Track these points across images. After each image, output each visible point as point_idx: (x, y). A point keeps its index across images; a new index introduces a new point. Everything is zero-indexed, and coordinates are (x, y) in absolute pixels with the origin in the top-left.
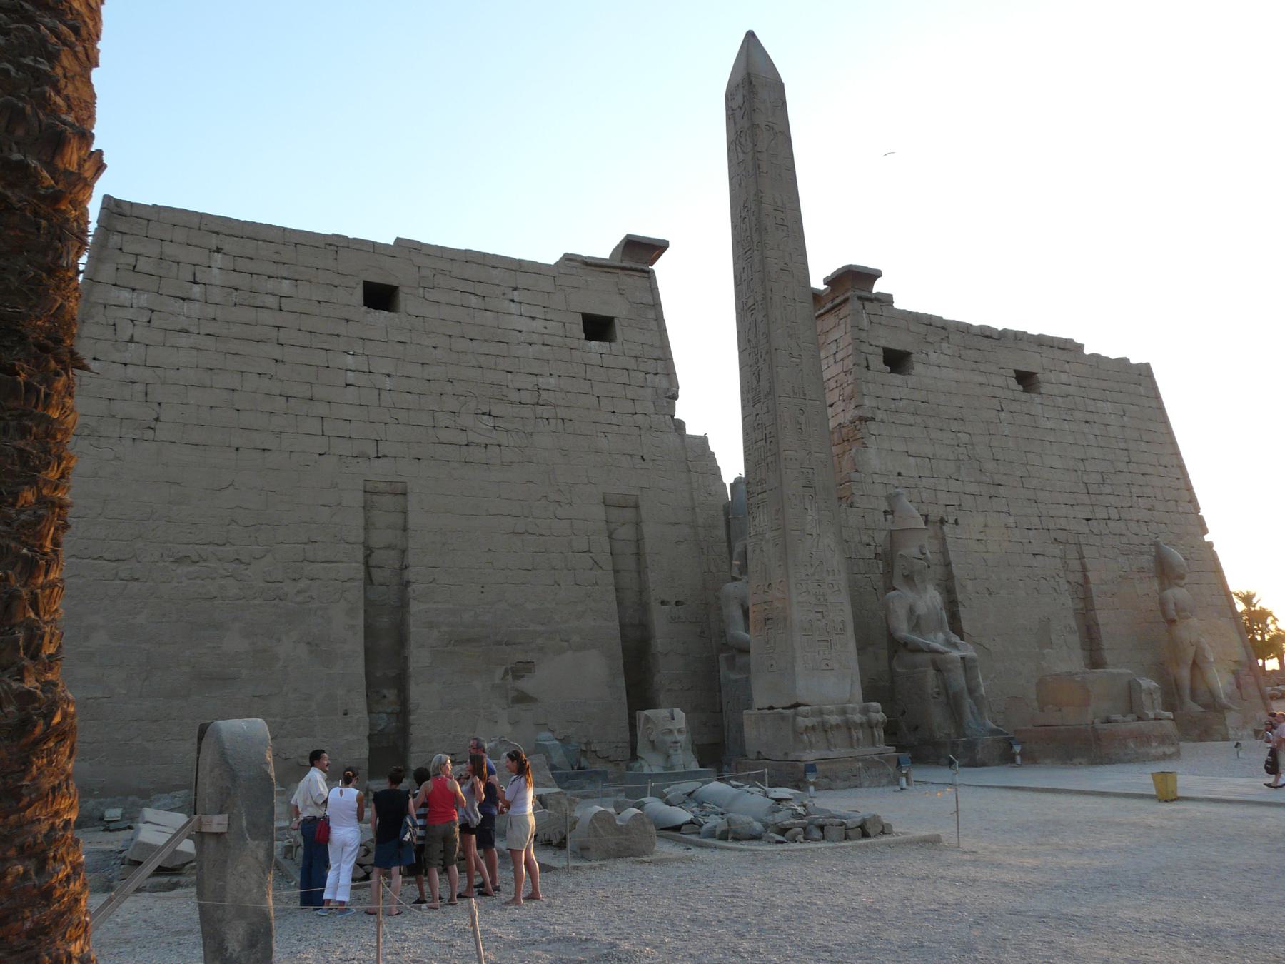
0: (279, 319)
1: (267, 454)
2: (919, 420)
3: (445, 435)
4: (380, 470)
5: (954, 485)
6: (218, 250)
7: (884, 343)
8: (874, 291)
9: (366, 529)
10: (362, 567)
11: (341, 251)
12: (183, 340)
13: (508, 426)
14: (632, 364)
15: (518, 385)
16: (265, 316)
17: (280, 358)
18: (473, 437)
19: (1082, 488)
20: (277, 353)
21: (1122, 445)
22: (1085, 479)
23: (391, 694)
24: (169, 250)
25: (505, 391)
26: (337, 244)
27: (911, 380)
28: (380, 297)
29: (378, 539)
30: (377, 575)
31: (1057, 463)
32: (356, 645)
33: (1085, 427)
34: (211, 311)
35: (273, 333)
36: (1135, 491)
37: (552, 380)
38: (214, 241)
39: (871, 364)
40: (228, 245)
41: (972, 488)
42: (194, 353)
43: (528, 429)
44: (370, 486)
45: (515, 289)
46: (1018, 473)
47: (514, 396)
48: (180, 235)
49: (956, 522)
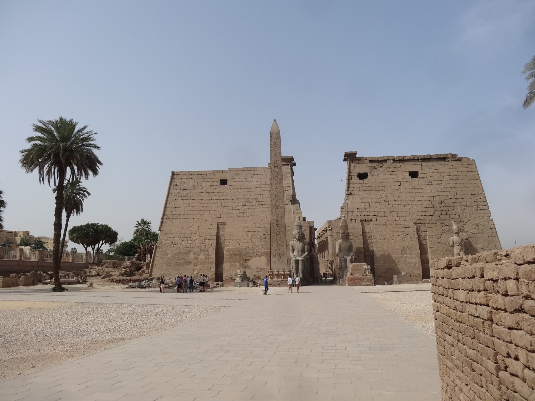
2: (367, 192)
3: (234, 211)
4: (221, 220)
5: (377, 210)
8: (357, 156)
12: (185, 198)
18: (241, 211)
21: (455, 190)
22: (433, 203)
24: (183, 180)
26: (214, 172)
27: (366, 181)
28: (224, 182)
31: (422, 199)
33: (437, 186)
36: (456, 204)
37: (261, 196)
38: (191, 177)
40: (193, 177)
41: (385, 210)
47: (251, 201)
48: (184, 177)
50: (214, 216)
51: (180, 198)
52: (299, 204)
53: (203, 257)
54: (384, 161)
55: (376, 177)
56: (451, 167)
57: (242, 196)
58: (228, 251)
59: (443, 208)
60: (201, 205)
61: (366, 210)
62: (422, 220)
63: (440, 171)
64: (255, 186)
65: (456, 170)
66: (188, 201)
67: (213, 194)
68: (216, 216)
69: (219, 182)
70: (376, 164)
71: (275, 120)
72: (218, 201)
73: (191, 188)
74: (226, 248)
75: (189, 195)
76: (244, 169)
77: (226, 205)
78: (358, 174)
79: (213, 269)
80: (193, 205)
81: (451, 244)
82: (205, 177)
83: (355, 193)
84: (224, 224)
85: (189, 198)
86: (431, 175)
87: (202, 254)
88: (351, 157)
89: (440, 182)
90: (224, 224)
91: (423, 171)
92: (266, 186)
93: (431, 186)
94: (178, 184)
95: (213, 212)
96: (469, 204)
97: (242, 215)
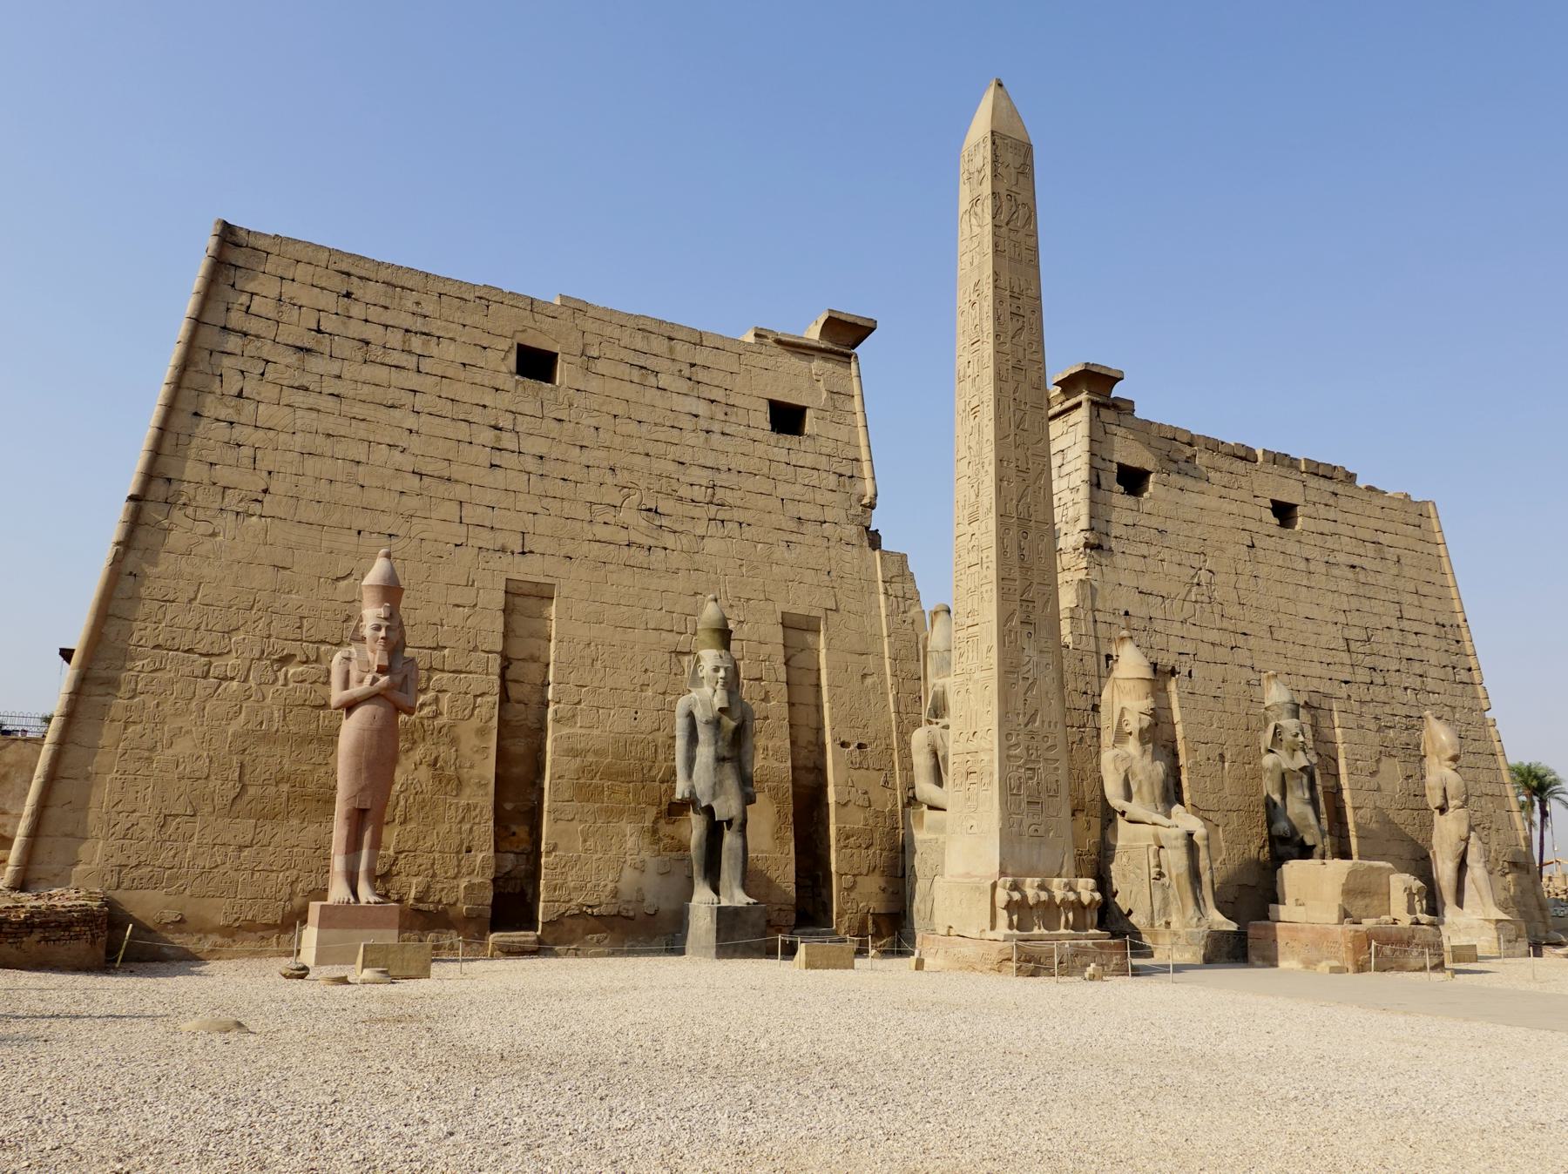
0: (414, 381)
1: (394, 540)
2: (1153, 550)
3: (602, 532)
4: (529, 570)
6: (348, 295)
9: (505, 636)
10: (495, 679)
11: (493, 307)
14: (823, 462)
15: (691, 480)
17: (415, 428)
19: (1342, 644)
20: (411, 422)
23: (522, 831)
24: (289, 290)
26: (487, 298)
28: (536, 364)
29: (516, 651)
30: (514, 691)
32: (488, 769)
33: (1350, 574)
34: (335, 367)
35: (407, 398)
36: (1408, 652)
37: (733, 477)
39: (1103, 482)
41: (1214, 636)
42: (314, 415)
43: (700, 531)
44: (512, 586)
46: (1268, 622)
47: (684, 491)
51: (269, 392)
53: (424, 773)
56: (1378, 512)
57: (639, 461)
58: (573, 753)
60: (406, 462)
61: (1158, 625)
62: (1326, 696)
63: (1351, 519)
66: (328, 424)
68: (500, 539)
69: (513, 357)
76: (645, 327)
78: (1120, 466)
79: (484, 854)
80: (359, 452)
82: (429, 307)
83: (1113, 544)
84: (544, 594)
87: (417, 754)
89: (1356, 561)
91: (1310, 510)
92: (752, 433)
93: (1335, 571)
97: (639, 556)
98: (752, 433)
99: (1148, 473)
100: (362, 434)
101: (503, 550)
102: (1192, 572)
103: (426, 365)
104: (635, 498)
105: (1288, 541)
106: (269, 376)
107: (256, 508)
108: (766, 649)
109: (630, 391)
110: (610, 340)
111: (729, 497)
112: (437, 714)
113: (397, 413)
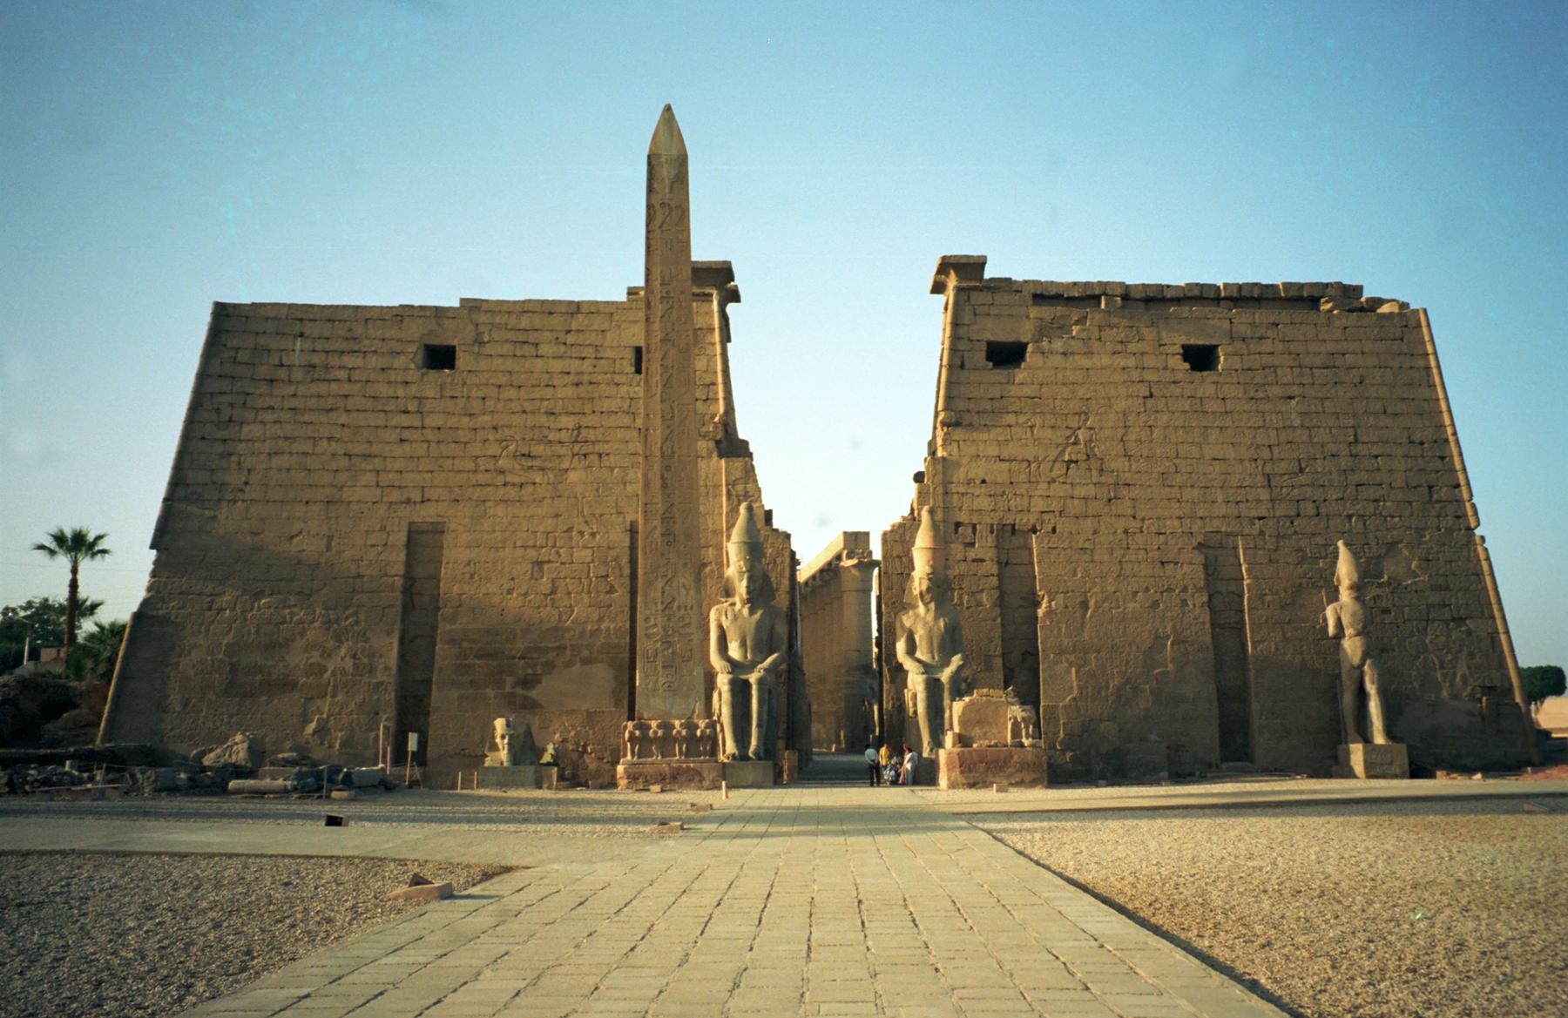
2: (1022, 419)
3: (481, 478)
4: (426, 514)
5: (1058, 489)
6: (302, 335)
7: (989, 336)
8: (987, 276)
11: (406, 321)
12: (269, 416)
13: (548, 465)
16: (334, 386)
21: (1351, 422)
22: (1268, 469)
24: (262, 341)
25: (546, 432)
26: (403, 314)
27: (1020, 375)
28: (440, 358)
31: (1230, 453)
34: (291, 390)
35: (341, 403)
38: (297, 328)
40: (309, 329)
41: (1088, 491)
45: (569, 332)
46: (1160, 469)
48: (270, 326)
49: (1054, 530)
50: (395, 496)
51: (250, 416)
52: (750, 455)
53: (349, 664)
54: (1086, 297)
55: (1057, 360)
56: (1338, 334)
57: (518, 420)
58: (452, 642)
59: (1308, 492)
60: (337, 448)
62: (1228, 535)
64: (571, 379)
65: (1354, 346)
67: (392, 406)
69: (420, 358)
70: (1059, 310)
71: (668, 109)
72: (416, 435)
73: (298, 375)
74: (444, 628)
75: (294, 403)
77: (448, 449)
78: (989, 344)
80: (306, 446)
81: (1331, 630)
83: (976, 419)
84: (438, 530)
85: (287, 416)
86: (1267, 360)
87: (343, 651)
88: (961, 275)
90: (438, 530)
92: (617, 378)
94: (241, 357)
95: (392, 478)
96: (1399, 481)
97: (512, 493)
98: (617, 378)
99: (1023, 347)
100: (310, 434)
101: (408, 501)
102: (1068, 433)
103: (356, 375)
104: (512, 448)
105: (1205, 383)
106: (249, 404)
107: (240, 495)
108: (613, 553)
109: (510, 364)
110: (499, 327)
111: (591, 435)
112: (357, 622)
113: (333, 415)
